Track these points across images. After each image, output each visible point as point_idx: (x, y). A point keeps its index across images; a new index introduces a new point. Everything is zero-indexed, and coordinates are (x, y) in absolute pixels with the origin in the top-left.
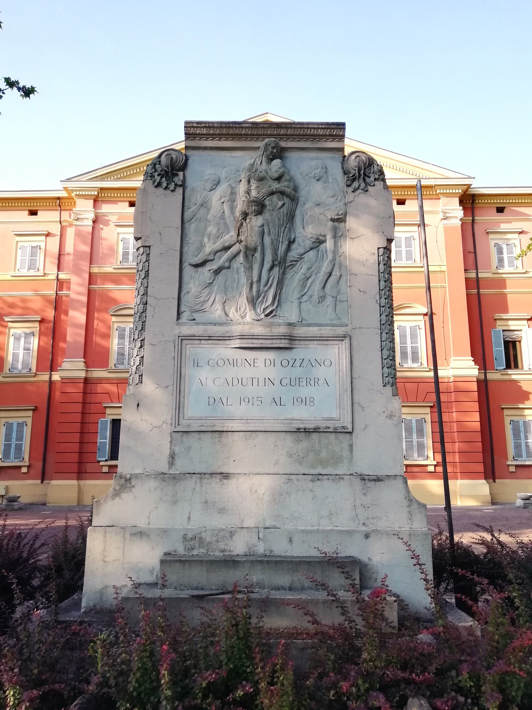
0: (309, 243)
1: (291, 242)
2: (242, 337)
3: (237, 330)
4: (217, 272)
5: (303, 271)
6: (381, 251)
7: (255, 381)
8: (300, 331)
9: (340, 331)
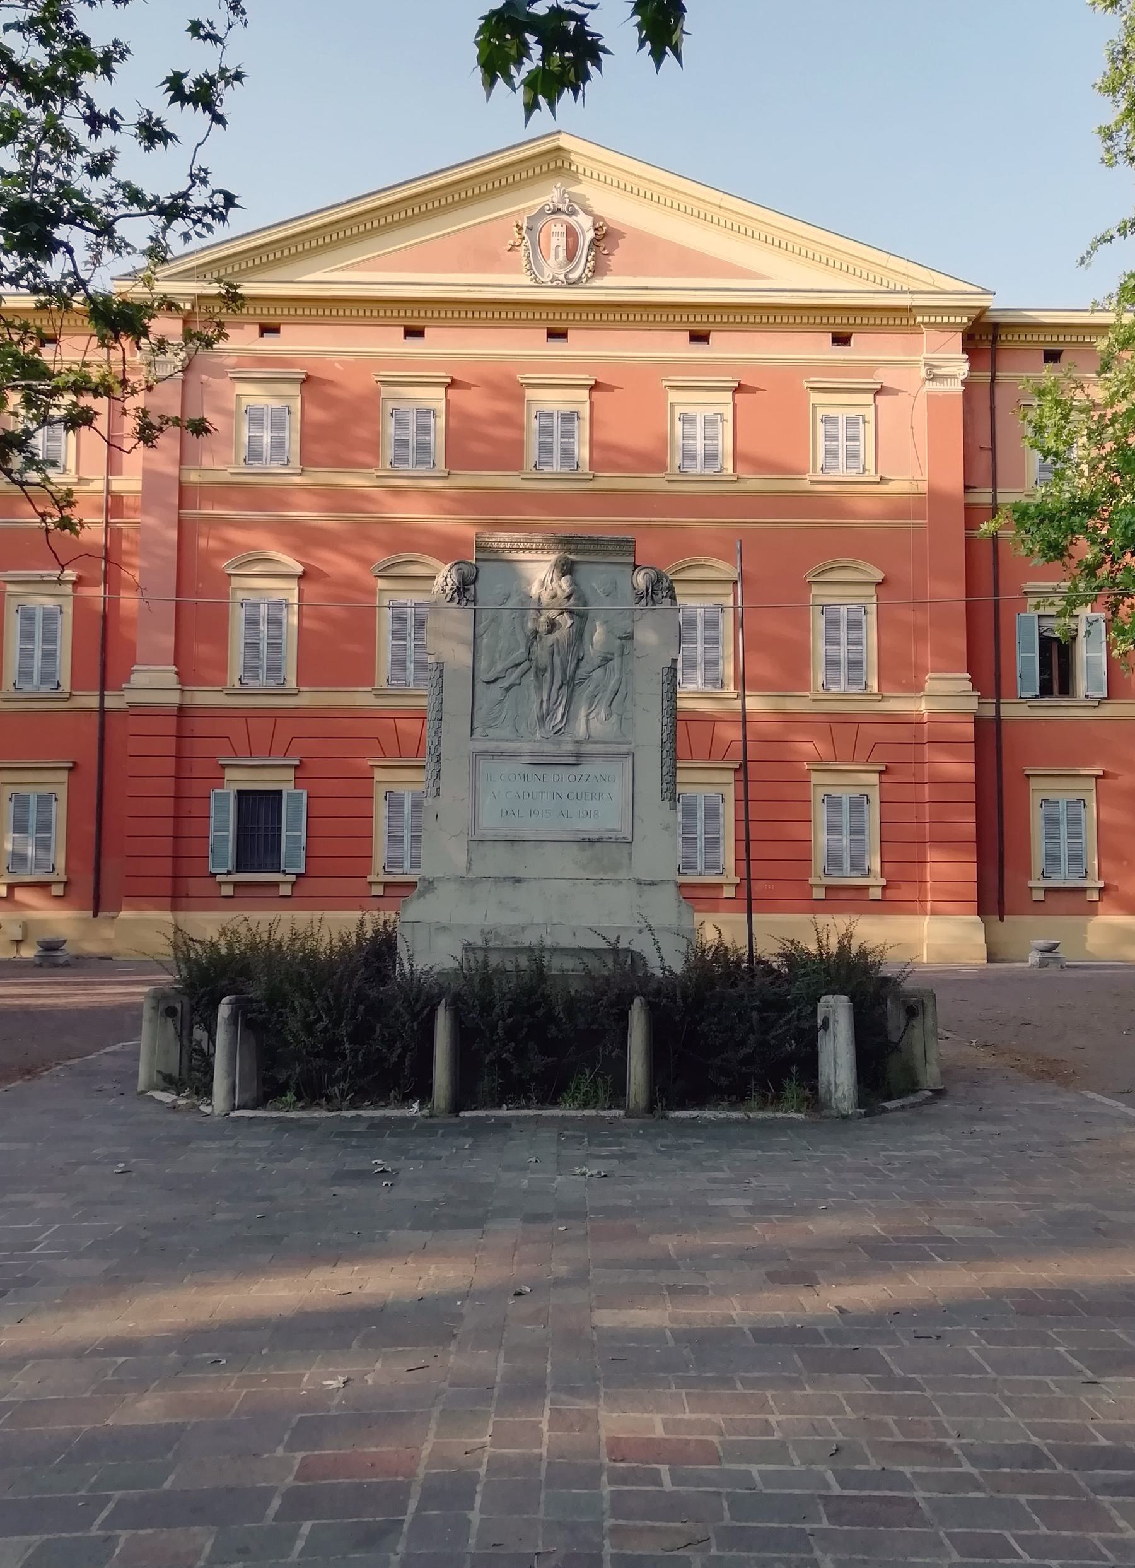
0: (597, 662)
1: (579, 660)
2: (532, 754)
3: (526, 747)
4: (508, 689)
5: (591, 688)
6: (666, 670)
7: (545, 795)
8: (587, 748)
9: (624, 748)
